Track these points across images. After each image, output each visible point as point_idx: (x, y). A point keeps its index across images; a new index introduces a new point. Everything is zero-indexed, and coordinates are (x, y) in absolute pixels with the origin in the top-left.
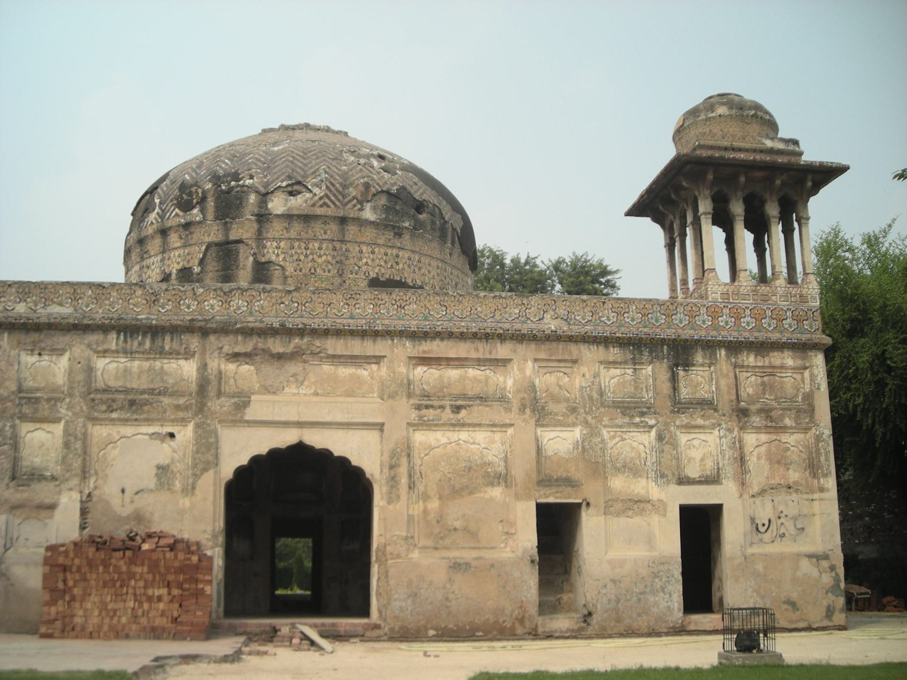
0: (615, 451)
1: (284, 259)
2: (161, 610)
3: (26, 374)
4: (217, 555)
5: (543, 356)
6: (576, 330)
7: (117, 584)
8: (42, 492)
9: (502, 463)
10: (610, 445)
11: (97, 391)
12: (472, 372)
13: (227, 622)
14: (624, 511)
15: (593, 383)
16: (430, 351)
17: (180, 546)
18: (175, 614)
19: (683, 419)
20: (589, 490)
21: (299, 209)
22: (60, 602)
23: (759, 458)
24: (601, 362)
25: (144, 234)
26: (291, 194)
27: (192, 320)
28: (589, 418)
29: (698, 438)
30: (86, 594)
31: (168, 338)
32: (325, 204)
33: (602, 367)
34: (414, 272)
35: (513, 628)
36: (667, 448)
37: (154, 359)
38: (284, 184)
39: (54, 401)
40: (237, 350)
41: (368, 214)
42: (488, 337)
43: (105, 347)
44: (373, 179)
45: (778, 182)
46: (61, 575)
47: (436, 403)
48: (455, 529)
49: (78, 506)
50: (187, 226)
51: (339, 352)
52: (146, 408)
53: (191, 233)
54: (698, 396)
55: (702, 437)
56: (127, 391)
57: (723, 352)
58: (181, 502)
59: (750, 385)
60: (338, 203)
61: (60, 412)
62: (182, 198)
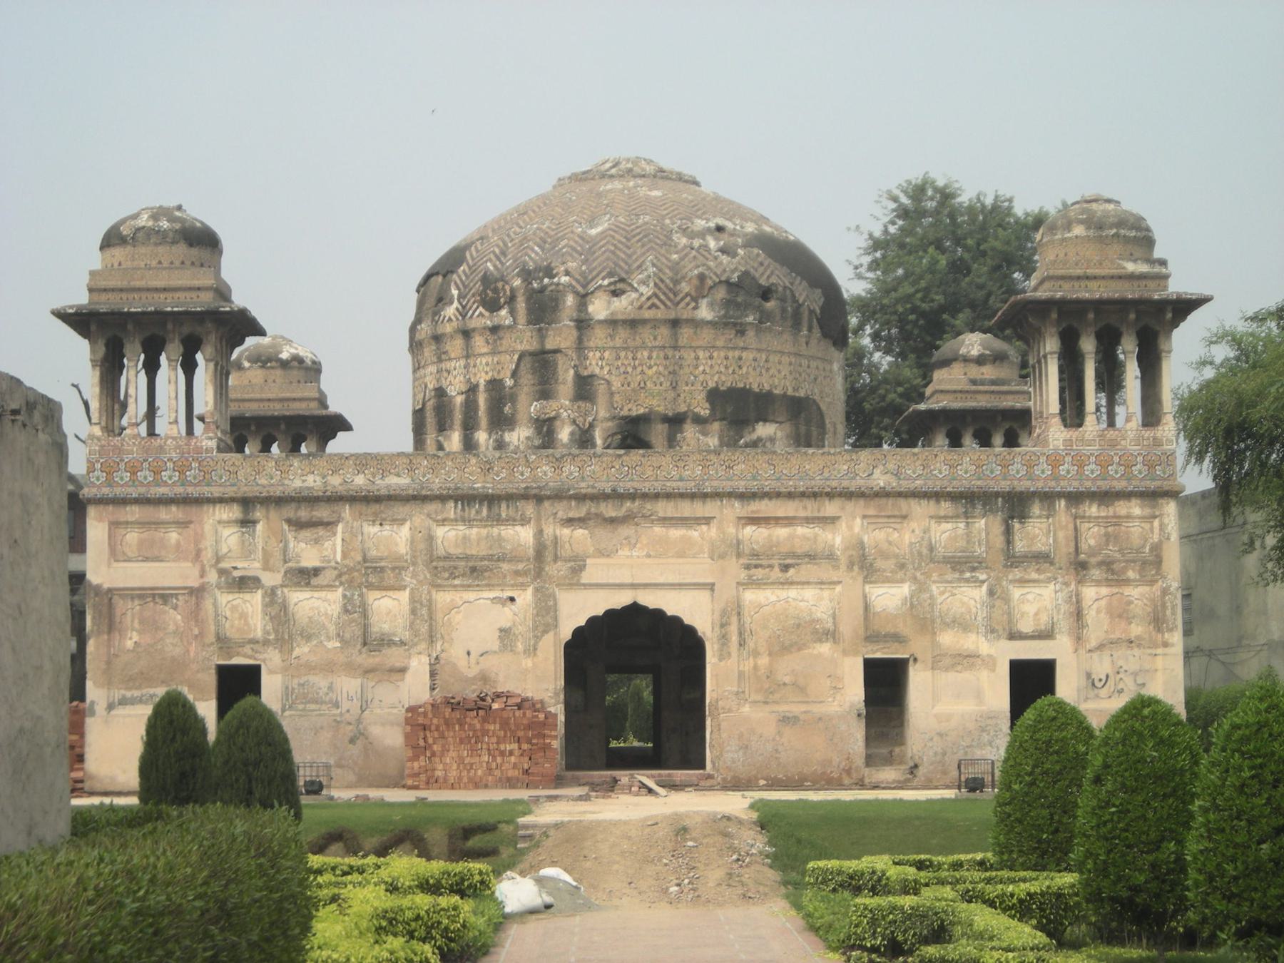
0: (944, 607)
1: (610, 372)
2: (513, 763)
3: (369, 544)
4: (558, 710)
5: (871, 512)
6: (906, 485)
7: (473, 741)
8: (393, 656)
9: (830, 620)
10: (939, 601)
11: (439, 558)
12: (800, 530)
13: (569, 774)
14: (951, 668)
15: (923, 538)
16: (758, 512)
17: (526, 704)
18: (526, 767)
19: (1017, 573)
20: (916, 646)
21: (624, 313)
22: (422, 758)
23: (1098, 612)
24: (931, 517)
25: (440, 331)
26: (616, 294)
27: (527, 488)
28: (918, 574)
29: (1032, 592)
30: (445, 750)
31: (504, 505)
32: (653, 305)
33: (933, 522)
34: (761, 375)
35: (840, 779)
36: (998, 603)
37: (492, 526)
38: (606, 282)
39: (398, 570)
40: (571, 515)
41: (705, 312)
42: (815, 495)
43: (445, 516)
44: (709, 268)
45: (1132, 316)
46: (421, 734)
47: (764, 562)
48: (785, 684)
49: (428, 668)
50: (495, 329)
51: (669, 515)
52: (486, 574)
53: (500, 339)
54: (1034, 549)
55: (1037, 591)
56: (467, 558)
57: (1063, 503)
58: (524, 662)
59: (1091, 536)
60: (669, 303)
61: (403, 580)
62: (486, 295)
